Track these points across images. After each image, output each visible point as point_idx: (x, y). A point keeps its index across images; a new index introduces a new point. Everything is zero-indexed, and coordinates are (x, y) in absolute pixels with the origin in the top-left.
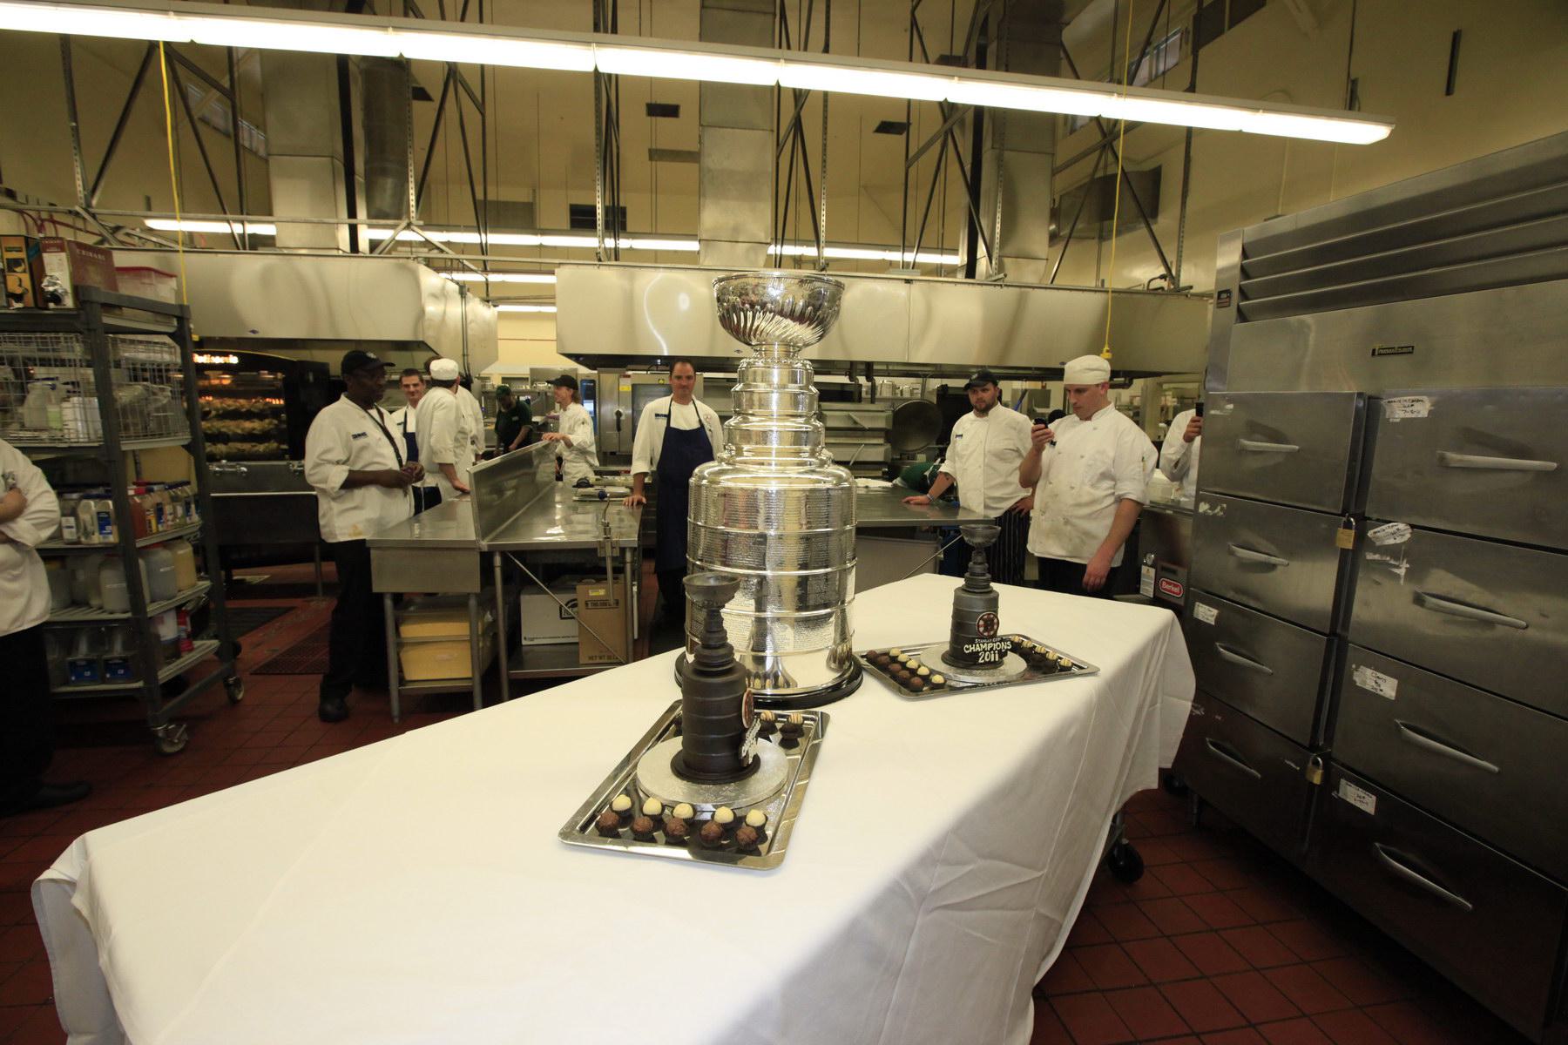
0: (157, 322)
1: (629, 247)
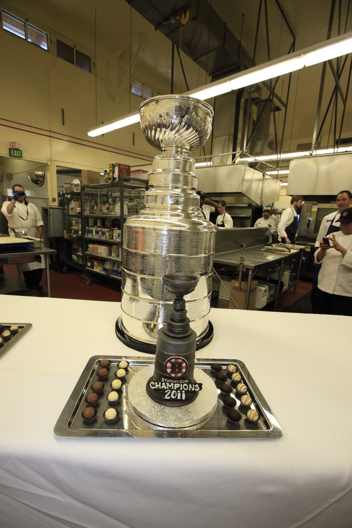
0: (141, 185)
1: (345, 151)
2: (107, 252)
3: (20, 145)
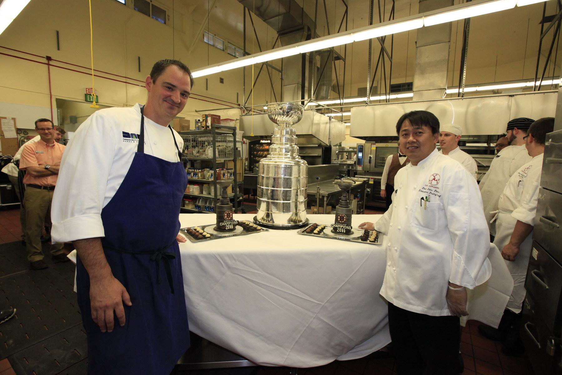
0: (229, 131)
2: (199, 191)
3: (96, 90)
